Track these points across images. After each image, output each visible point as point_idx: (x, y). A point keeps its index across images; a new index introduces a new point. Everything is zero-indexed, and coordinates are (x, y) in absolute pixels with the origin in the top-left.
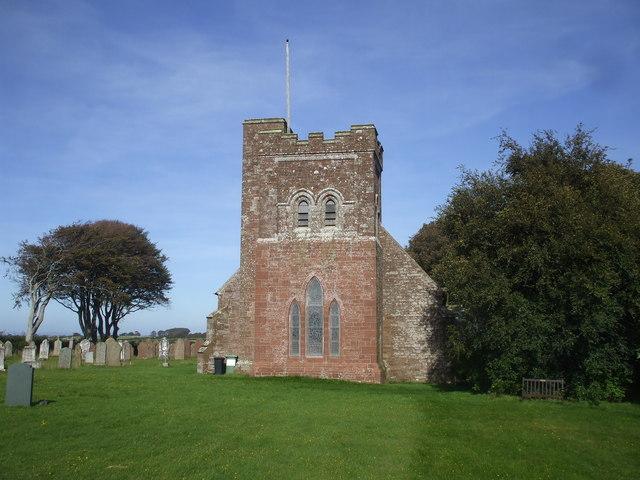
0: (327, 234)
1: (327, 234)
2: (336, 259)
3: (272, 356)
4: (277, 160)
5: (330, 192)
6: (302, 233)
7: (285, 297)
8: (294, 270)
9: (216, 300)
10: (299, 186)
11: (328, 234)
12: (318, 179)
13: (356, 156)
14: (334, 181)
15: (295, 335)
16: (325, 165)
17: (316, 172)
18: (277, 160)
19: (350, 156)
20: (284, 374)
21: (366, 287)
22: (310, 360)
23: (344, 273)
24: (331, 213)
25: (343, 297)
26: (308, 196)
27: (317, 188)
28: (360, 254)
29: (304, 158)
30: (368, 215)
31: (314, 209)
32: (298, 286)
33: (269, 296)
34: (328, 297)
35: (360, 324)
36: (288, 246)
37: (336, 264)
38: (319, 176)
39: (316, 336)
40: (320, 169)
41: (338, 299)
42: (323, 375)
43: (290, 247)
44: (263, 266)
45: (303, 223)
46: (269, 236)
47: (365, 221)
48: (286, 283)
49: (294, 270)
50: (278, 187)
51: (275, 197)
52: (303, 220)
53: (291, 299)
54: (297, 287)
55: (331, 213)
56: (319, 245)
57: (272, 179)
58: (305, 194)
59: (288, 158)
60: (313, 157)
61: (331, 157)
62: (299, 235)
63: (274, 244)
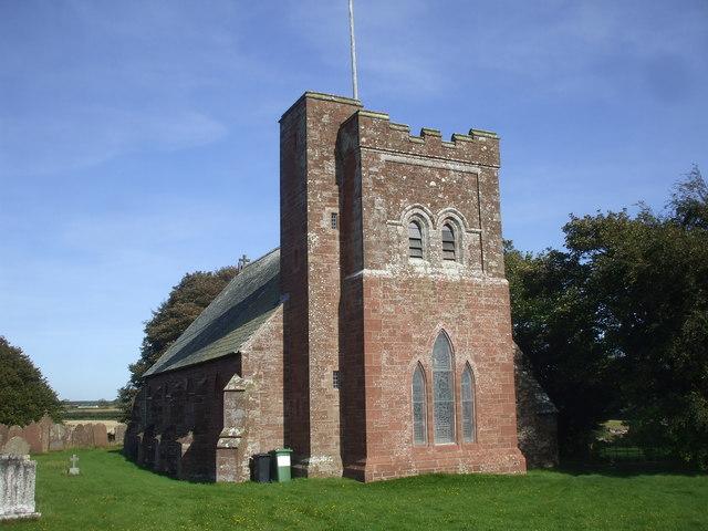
0: (452, 271)
1: (452, 271)
2: (468, 306)
3: (391, 446)
4: (384, 157)
5: (451, 214)
6: (420, 266)
7: (406, 358)
8: (417, 319)
9: (128, 375)
10: (412, 200)
11: (452, 271)
12: (437, 191)
13: (479, 171)
14: (454, 199)
15: (418, 412)
16: (443, 176)
17: (433, 183)
18: (384, 157)
19: (475, 169)
20: (413, 472)
21: (502, 346)
22: (441, 449)
23: (477, 325)
24: (449, 245)
25: (476, 359)
26: (424, 214)
27: (435, 206)
28: (492, 301)
29: (419, 162)
30: (496, 250)
31: (434, 234)
32: (422, 343)
33: (385, 356)
34: (461, 358)
35: (496, 396)
36: (406, 284)
37: (466, 313)
38: (437, 191)
39: (447, 413)
40: (438, 181)
41: (472, 363)
42: (462, 469)
43: (410, 284)
44: (375, 311)
45: (415, 253)
46: (378, 267)
47: (494, 258)
48: (407, 338)
49: (417, 319)
50: (387, 196)
51: (383, 210)
52: (417, 249)
53: (414, 362)
54: (420, 344)
55: (449, 245)
56: (445, 285)
57: (378, 184)
58: (420, 212)
59: (398, 158)
60: (429, 163)
61: (452, 167)
62: (417, 270)
63: (389, 280)
